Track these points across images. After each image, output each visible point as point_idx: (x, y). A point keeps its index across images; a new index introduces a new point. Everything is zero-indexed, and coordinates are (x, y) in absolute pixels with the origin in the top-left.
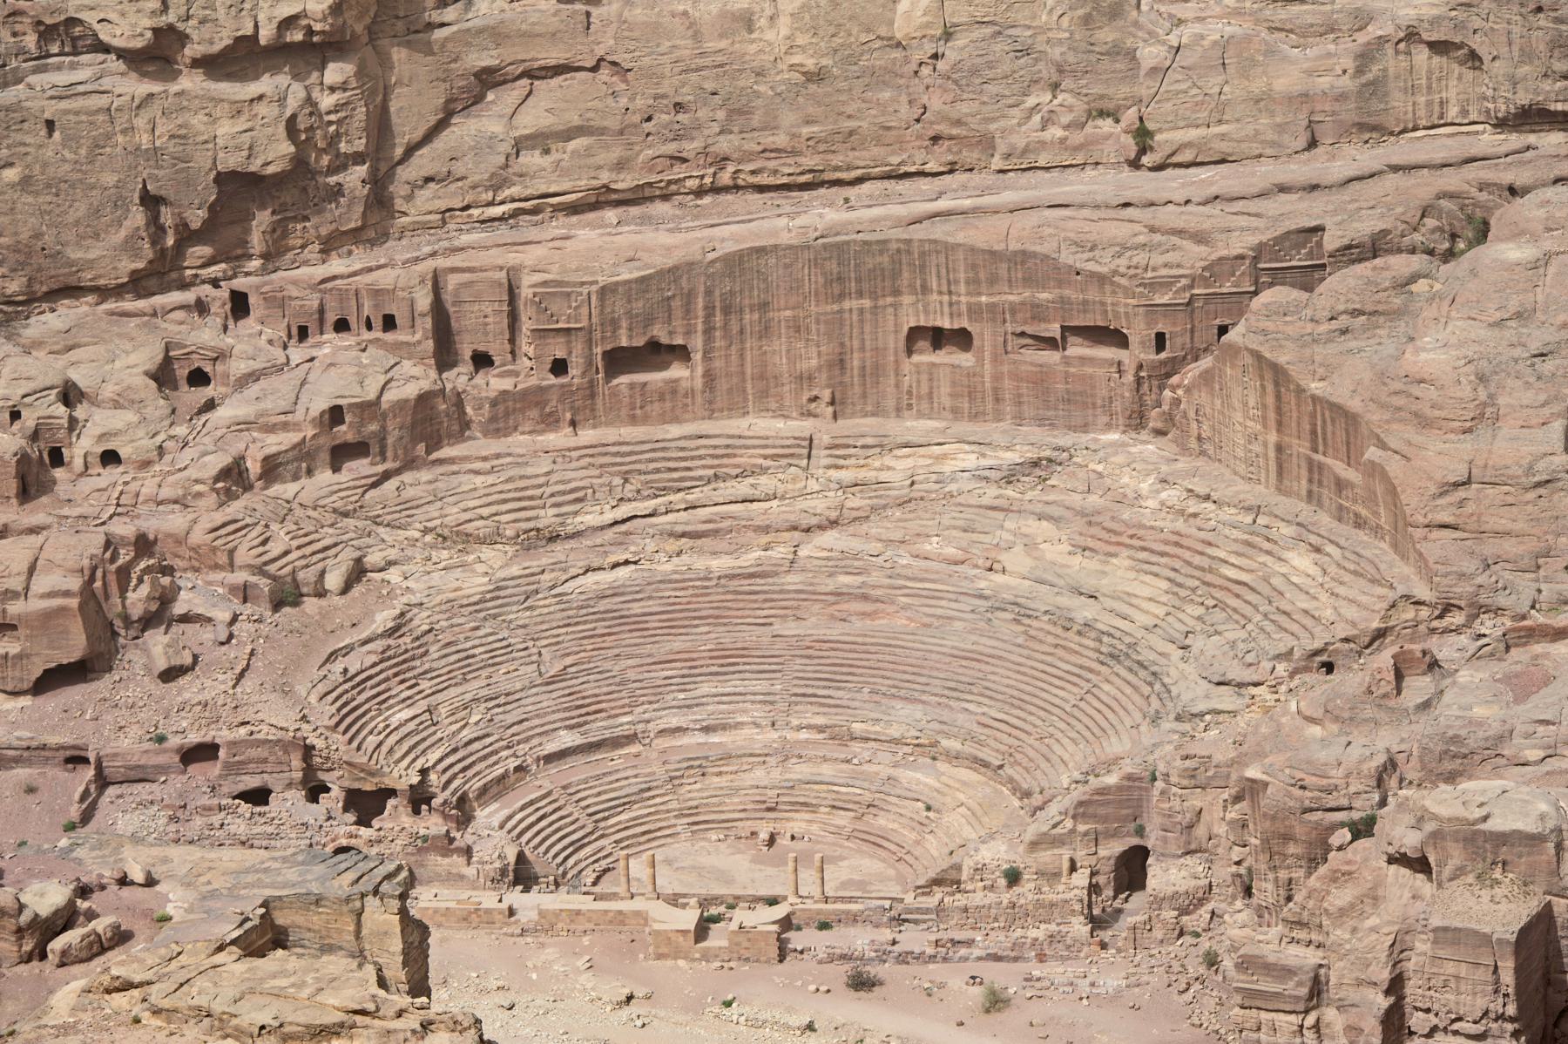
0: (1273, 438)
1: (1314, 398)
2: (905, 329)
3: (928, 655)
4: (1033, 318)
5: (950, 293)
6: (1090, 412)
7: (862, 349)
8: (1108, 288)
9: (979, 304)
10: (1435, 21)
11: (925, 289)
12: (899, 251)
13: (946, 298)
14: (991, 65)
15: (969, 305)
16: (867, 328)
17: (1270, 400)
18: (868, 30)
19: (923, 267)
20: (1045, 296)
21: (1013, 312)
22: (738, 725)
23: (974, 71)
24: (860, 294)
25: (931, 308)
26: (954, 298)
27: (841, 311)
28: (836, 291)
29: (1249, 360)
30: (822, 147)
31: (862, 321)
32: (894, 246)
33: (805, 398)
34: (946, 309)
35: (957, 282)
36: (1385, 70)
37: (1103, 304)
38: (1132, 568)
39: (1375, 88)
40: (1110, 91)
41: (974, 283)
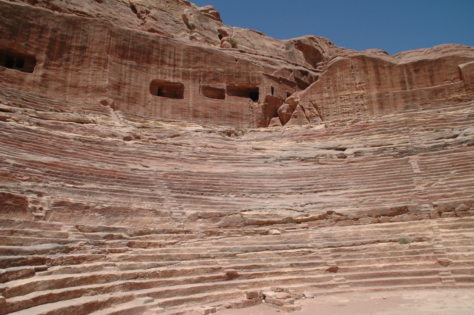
0: (374, 92)
1: (401, 66)
2: (151, 80)
3: (259, 180)
4: (214, 80)
5: (174, 66)
6: (240, 122)
7: (129, 84)
8: (250, 67)
9: (189, 72)
10: (304, 40)
12: (153, 41)
16: (133, 75)
17: (372, 74)
19: (163, 51)
21: (205, 76)
24: (132, 58)
26: (176, 68)
29: (354, 62)
30: (103, 18)
32: (151, 39)
33: (99, 100)
34: (172, 73)
37: (248, 73)
38: (348, 139)
39: (291, 54)
40: (211, 37)
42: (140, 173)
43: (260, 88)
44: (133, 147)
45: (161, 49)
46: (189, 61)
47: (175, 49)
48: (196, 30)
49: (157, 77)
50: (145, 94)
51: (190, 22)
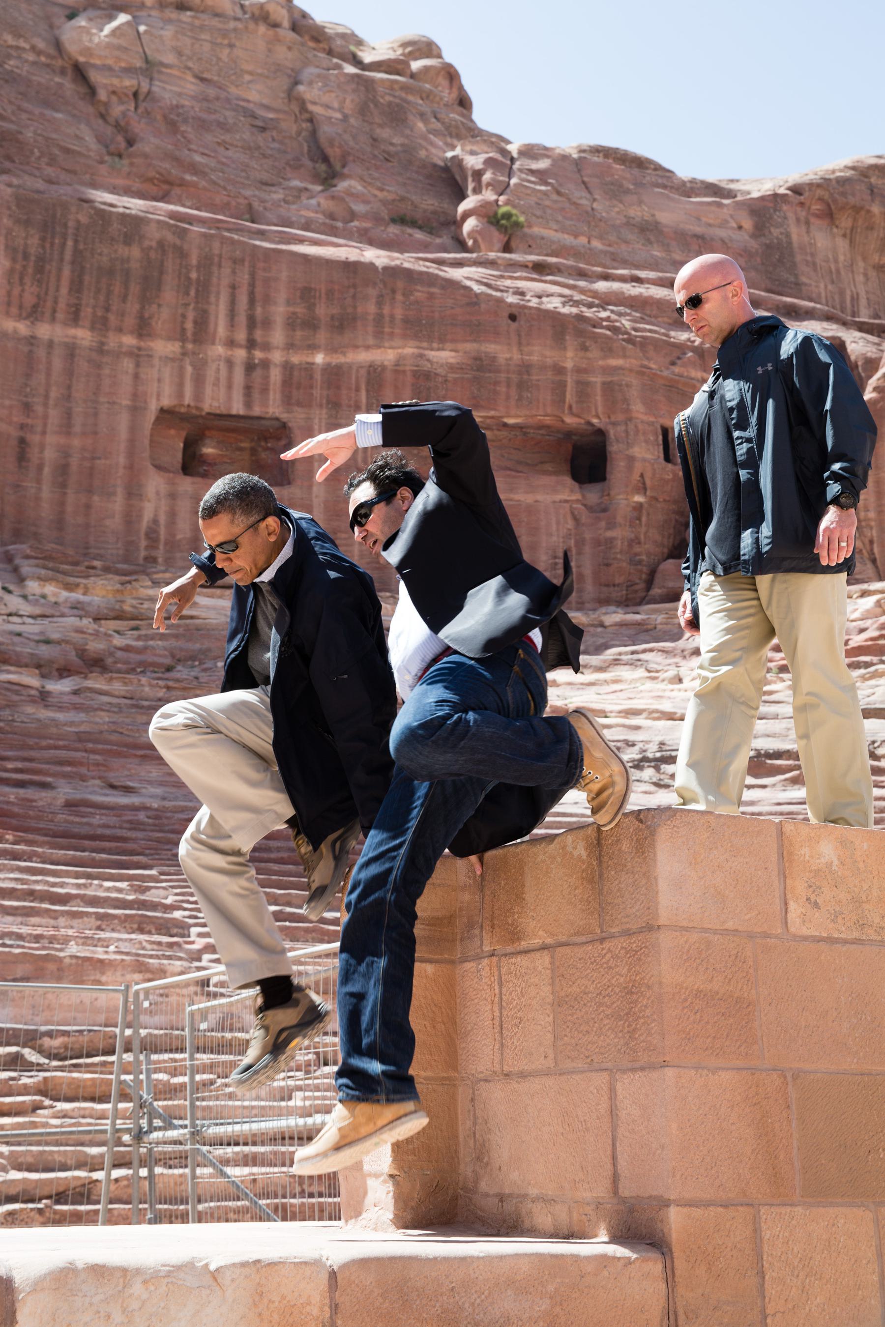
2: (153, 407)
5: (251, 344)
8: (571, 341)
9: (309, 368)
11: (201, 333)
13: (240, 354)
14: (223, 126)
15: (288, 368)
18: (18, 36)
20: (443, 356)
22: (86, 970)
23: (203, 125)
24: (75, 318)
25: (210, 374)
26: (258, 354)
27: (32, 340)
28: (29, 299)
31: (70, 373)
35: (267, 324)
36: (788, 235)
37: (559, 370)
41: (304, 325)
42: (96, 820)
43: (612, 432)
44: (77, 708)
45: (194, 275)
46: (311, 324)
47: (253, 276)
48: (352, 168)
49: (180, 394)
50: (130, 467)
51: (326, 131)
